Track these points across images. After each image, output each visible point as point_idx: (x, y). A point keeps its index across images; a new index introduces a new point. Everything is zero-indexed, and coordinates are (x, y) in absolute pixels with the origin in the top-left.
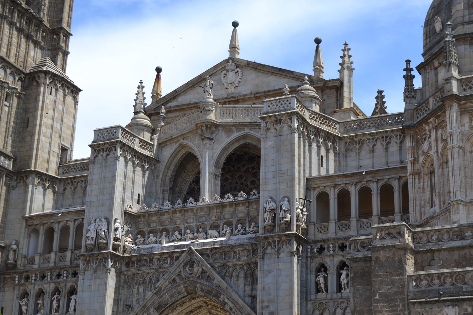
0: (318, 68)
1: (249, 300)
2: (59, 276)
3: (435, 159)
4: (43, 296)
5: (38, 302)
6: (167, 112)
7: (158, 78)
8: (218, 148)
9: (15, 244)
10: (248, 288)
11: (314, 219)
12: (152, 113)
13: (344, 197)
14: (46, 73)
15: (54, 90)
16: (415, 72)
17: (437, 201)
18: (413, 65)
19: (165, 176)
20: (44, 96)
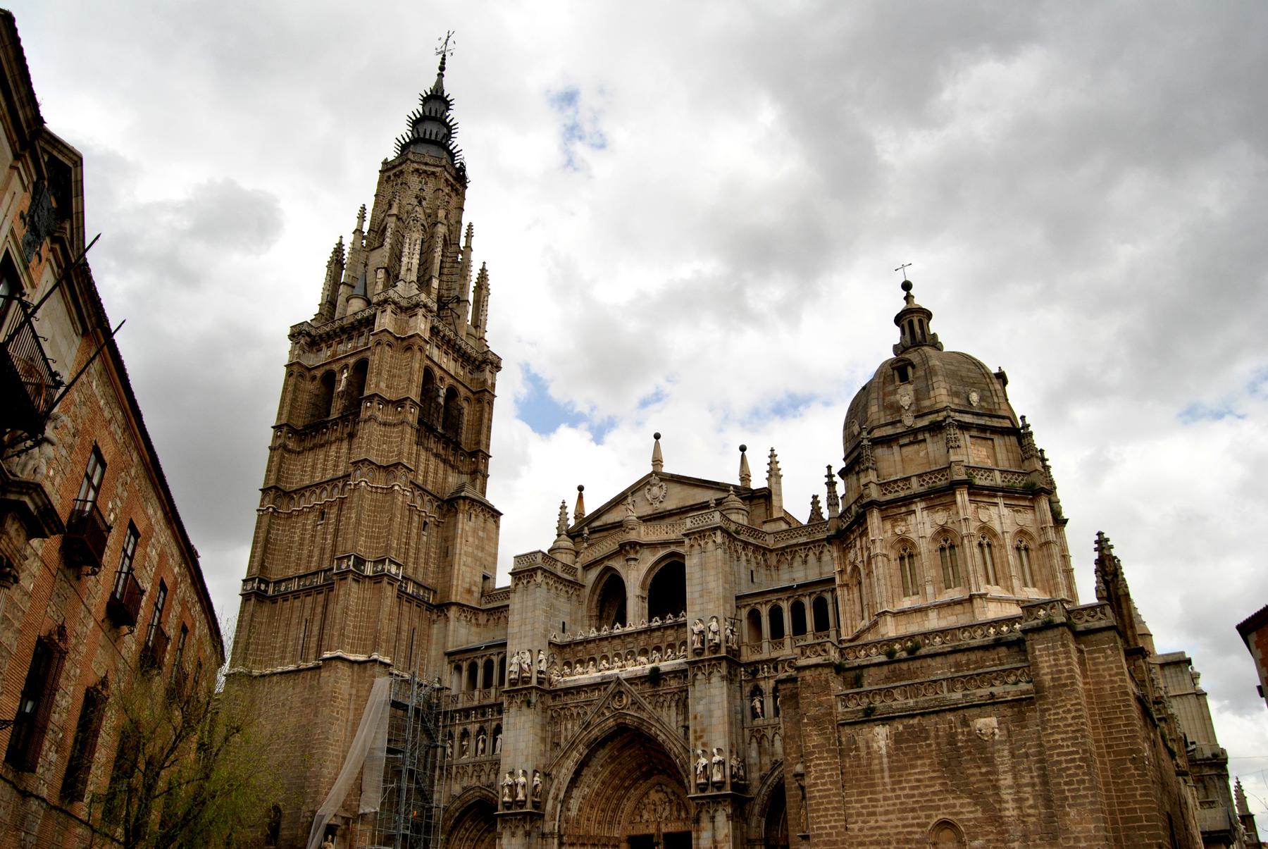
0: (745, 477)
1: (681, 731)
2: (483, 715)
3: (861, 566)
6: (591, 533)
7: (581, 497)
8: (644, 568)
10: (680, 718)
11: (746, 639)
12: (574, 535)
13: (776, 614)
14: (465, 498)
16: (837, 478)
17: (866, 614)
18: (835, 471)
19: (590, 601)
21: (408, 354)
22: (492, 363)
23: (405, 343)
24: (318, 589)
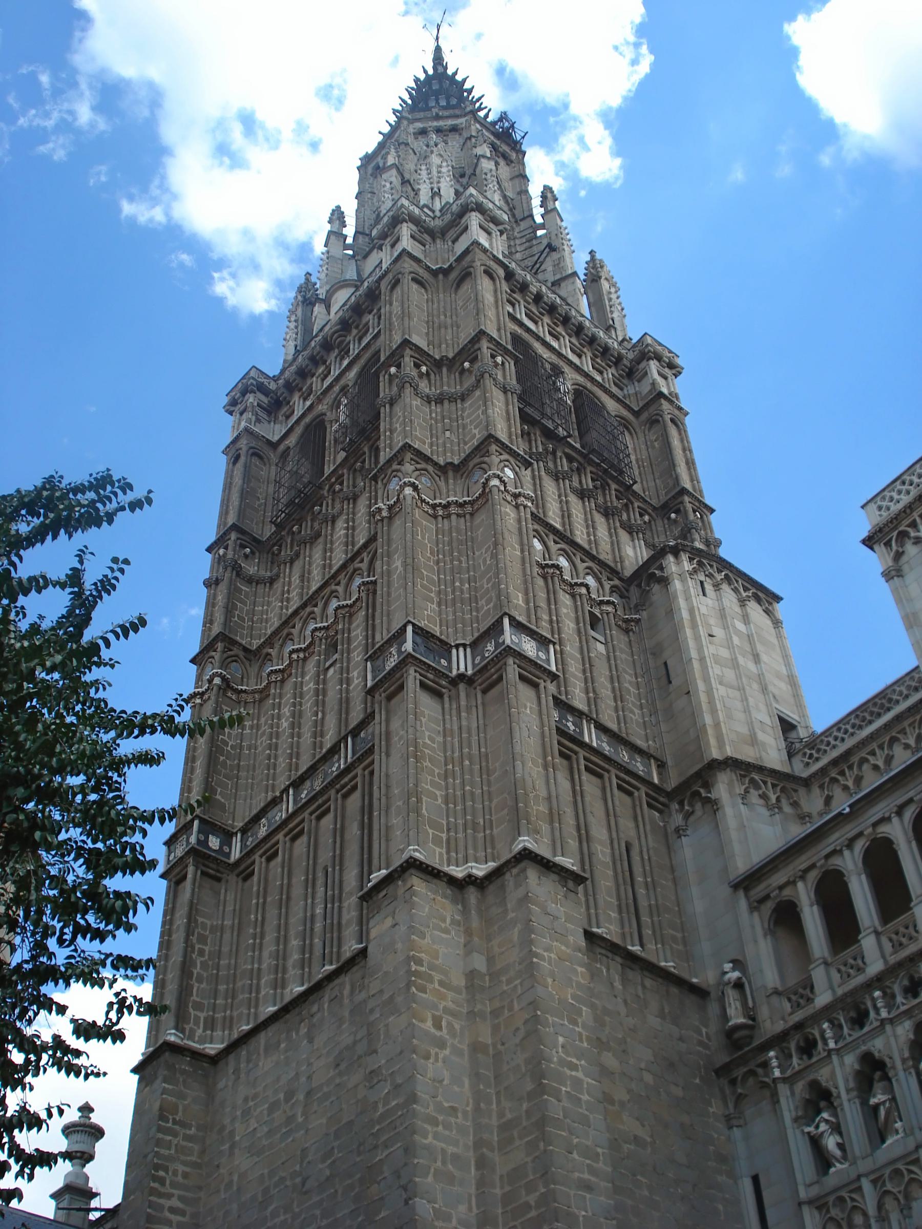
4: (886, 1078)
5: (873, 1101)
9: (734, 969)
15: (708, 587)
20: (688, 598)
21: (466, 287)
22: (659, 358)
23: (453, 275)
24: (343, 784)
